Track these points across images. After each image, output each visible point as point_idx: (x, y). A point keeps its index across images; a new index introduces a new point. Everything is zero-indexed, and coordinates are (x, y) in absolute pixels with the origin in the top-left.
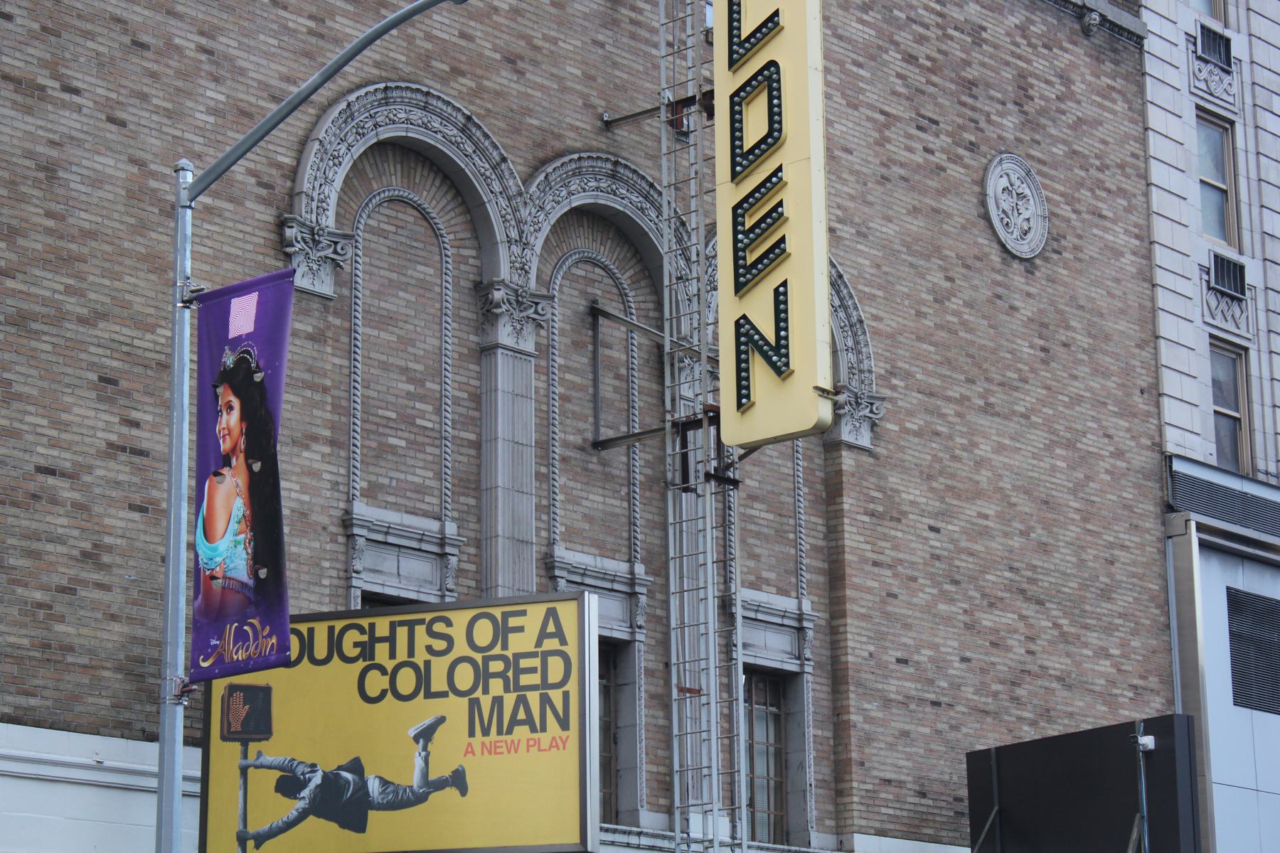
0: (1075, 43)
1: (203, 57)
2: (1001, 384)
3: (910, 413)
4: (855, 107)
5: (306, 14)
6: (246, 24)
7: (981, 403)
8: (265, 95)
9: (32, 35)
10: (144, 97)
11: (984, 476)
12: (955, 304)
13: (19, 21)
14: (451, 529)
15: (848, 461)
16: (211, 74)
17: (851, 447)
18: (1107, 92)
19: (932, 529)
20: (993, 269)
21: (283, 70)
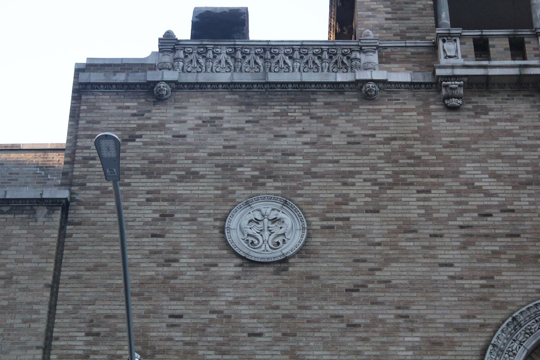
1: (401, 320)
5: (478, 277)
6: (431, 295)
8: (451, 329)
9: (277, 340)
13: (267, 335)
16: (408, 328)
21: (465, 312)
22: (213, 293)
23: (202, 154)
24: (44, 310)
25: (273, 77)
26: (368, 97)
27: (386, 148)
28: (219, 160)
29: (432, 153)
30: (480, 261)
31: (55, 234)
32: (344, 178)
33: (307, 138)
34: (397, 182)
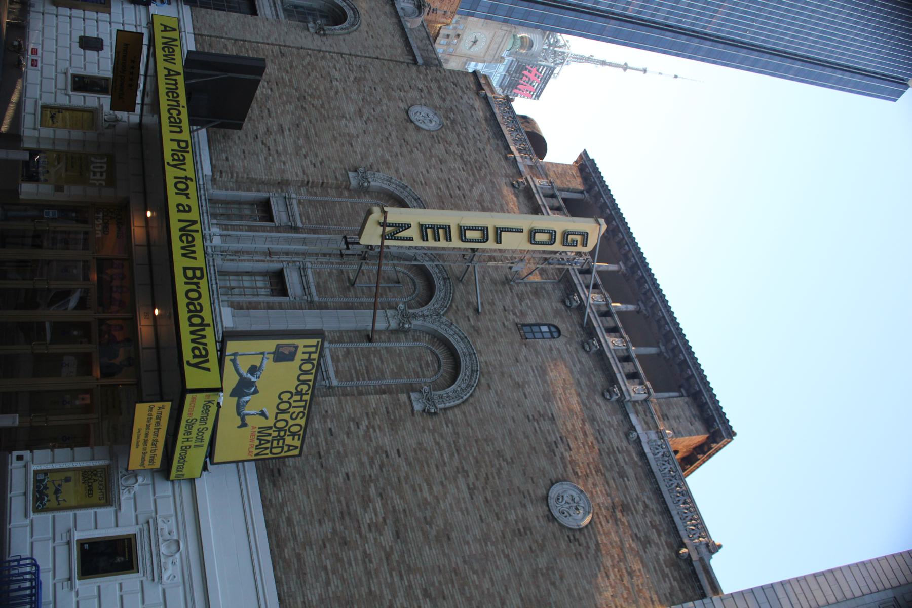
0: (668, 547)
2: (487, 500)
3: (441, 436)
4: (544, 400)
7: (471, 486)
10: (375, 138)
11: (436, 489)
12: (504, 464)
14: (300, 225)
15: (403, 397)
17: (409, 398)
18: (664, 576)
19: (398, 451)
20: (534, 491)
22: (389, 100)
23: (455, 103)
24: (367, 55)
25: (503, 127)
26: (506, 158)
27: (481, 160)
28: (454, 108)
29: (485, 176)
30: (434, 183)
31: (402, 60)
32: (460, 144)
33: (477, 136)
34: (465, 163)
